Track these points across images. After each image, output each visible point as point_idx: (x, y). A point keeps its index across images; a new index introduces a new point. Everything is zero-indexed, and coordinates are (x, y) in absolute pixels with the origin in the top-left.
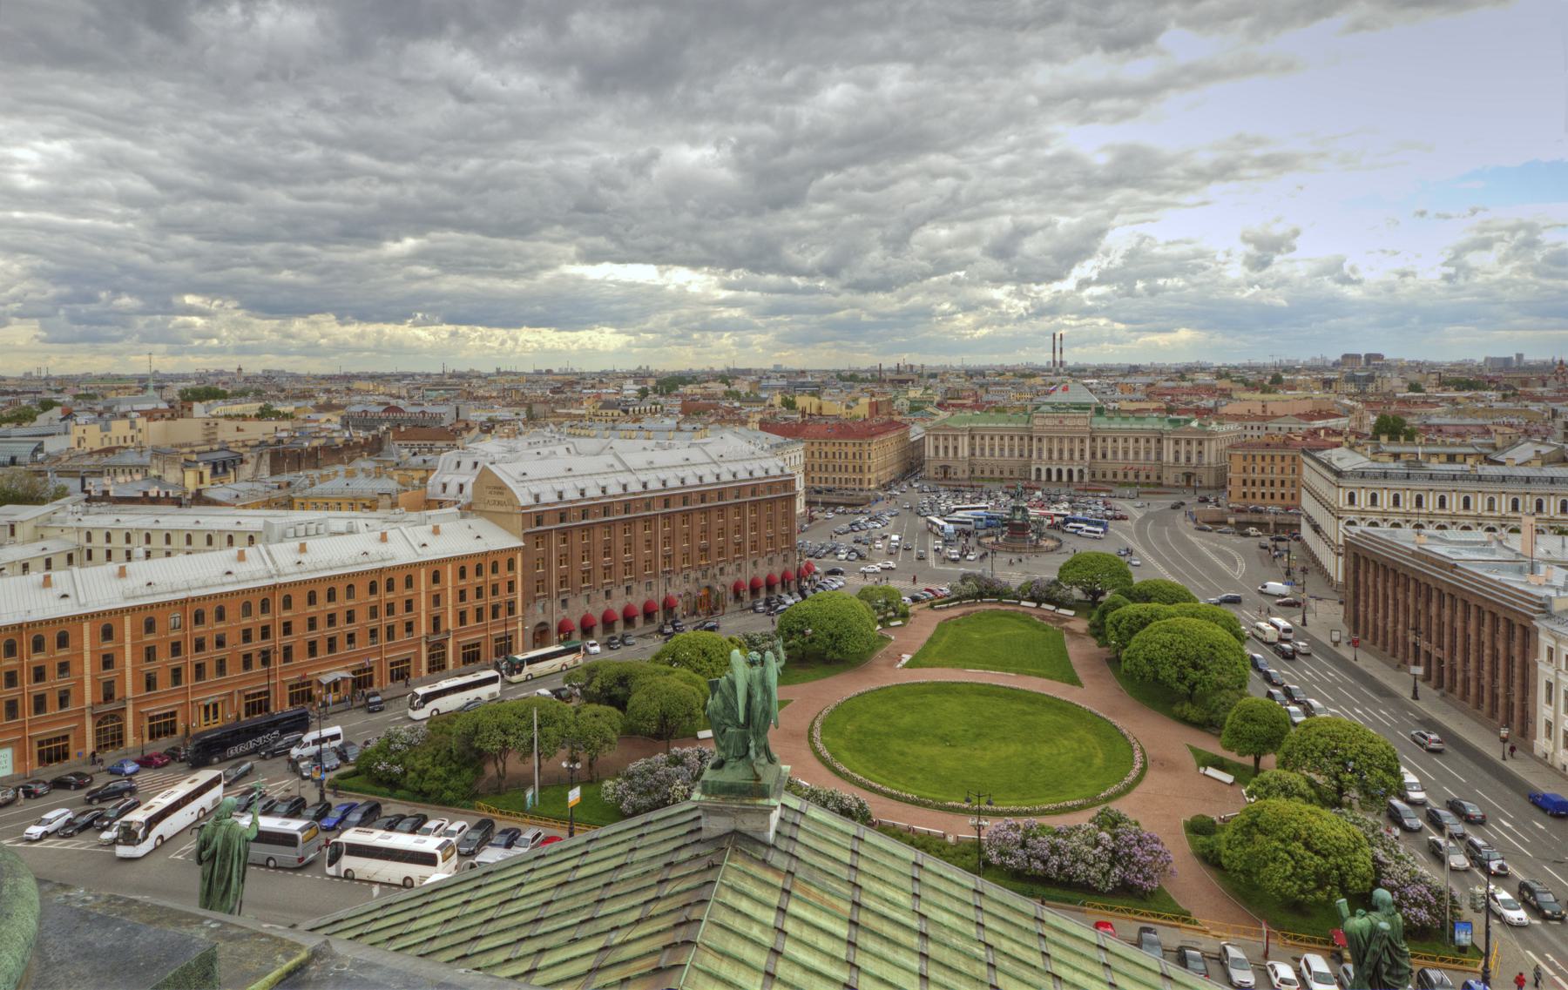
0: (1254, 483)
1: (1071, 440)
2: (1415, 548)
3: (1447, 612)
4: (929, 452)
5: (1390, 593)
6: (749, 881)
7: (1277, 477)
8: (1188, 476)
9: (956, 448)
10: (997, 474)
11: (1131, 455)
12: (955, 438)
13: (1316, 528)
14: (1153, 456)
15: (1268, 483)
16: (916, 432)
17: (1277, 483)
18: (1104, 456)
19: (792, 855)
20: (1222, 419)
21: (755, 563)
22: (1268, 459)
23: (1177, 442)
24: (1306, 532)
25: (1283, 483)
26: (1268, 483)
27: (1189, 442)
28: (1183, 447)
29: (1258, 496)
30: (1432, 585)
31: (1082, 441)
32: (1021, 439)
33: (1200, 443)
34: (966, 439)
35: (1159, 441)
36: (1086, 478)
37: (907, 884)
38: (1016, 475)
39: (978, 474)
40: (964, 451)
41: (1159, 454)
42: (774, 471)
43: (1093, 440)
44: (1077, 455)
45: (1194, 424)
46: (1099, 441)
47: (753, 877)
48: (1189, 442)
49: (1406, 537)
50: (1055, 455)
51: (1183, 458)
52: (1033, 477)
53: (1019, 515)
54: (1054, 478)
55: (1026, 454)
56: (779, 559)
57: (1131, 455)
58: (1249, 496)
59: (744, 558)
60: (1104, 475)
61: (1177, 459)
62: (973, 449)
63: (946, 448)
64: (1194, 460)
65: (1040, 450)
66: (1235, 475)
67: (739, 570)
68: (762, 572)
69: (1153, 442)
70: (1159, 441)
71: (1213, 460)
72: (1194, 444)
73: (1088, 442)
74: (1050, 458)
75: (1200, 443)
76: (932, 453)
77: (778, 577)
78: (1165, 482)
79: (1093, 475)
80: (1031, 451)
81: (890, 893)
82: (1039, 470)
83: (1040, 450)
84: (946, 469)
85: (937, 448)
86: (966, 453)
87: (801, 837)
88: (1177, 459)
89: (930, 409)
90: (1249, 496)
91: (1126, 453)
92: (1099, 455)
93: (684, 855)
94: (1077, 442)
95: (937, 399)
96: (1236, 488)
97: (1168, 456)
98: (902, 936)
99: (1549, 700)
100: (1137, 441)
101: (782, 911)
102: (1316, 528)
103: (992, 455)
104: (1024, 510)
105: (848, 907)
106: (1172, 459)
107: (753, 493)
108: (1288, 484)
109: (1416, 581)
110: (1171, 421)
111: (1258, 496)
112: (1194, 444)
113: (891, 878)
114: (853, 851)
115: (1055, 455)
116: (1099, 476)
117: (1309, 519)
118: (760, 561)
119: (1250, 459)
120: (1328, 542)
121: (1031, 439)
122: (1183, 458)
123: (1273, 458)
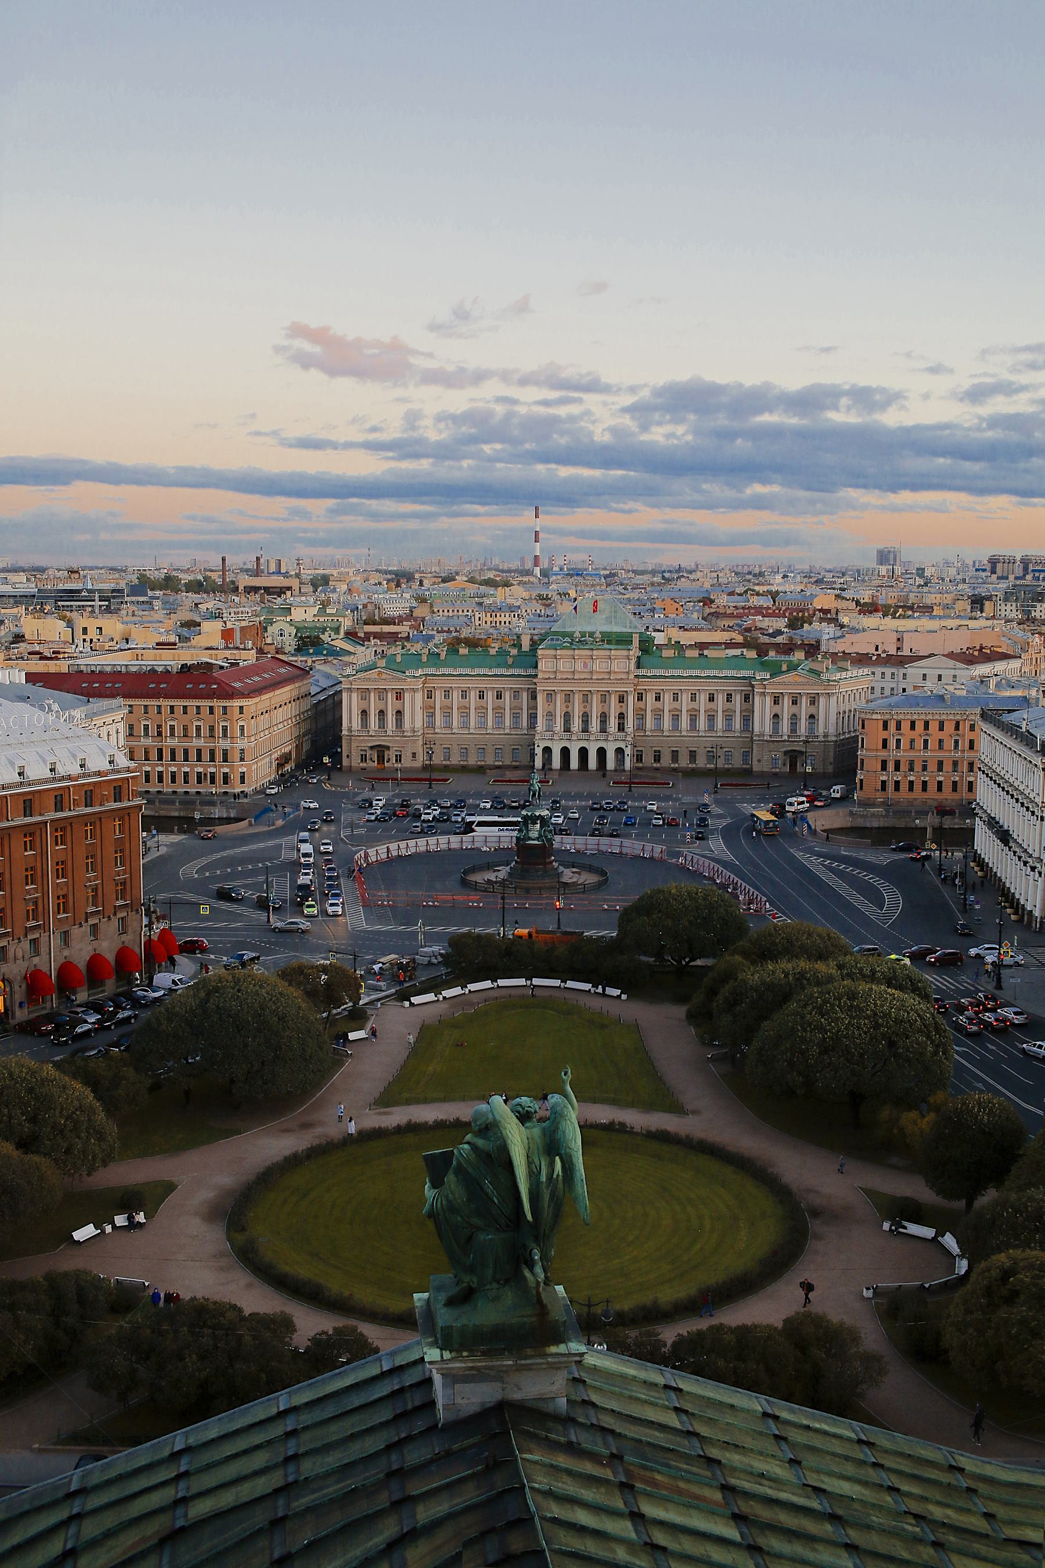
0: (897, 768)
1: (604, 697)
4: (350, 720)
6: (565, 1478)
7: (932, 755)
8: (793, 756)
11: (702, 723)
12: (399, 695)
13: (1005, 837)
14: (737, 723)
15: (918, 767)
17: (932, 767)
19: (603, 1429)
21: (66, 936)
22: (920, 726)
23: (776, 701)
24: (985, 842)
25: (940, 764)
28: (786, 708)
29: (904, 787)
31: (621, 700)
32: (516, 693)
33: (813, 701)
34: (419, 696)
36: (628, 765)
37: (771, 1446)
41: (747, 719)
42: (98, 763)
44: (613, 724)
47: (569, 1473)
50: (576, 725)
51: (785, 727)
52: (538, 763)
53: (535, 831)
54: (574, 764)
55: (525, 724)
56: (110, 928)
57: (702, 723)
58: (890, 787)
59: (45, 928)
63: (382, 713)
65: (550, 715)
66: (869, 754)
67: (37, 953)
68: (81, 952)
69: (738, 699)
71: (832, 730)
72: (804, 701)
73: (631, 699)
74: (567, 730)
76: (356, 724)
77: (111, 957)
78: (756, 768)
79: (639, 758)
81: (760, 1465)
82: (547, 750)
83: (550, 715)
84: (381, 750)
85: (364, 713)
86: (419, 724)
87: (595, 1398)
89: (340, 644)
90: (890, 787)
91: (693, 718)
93: (414, 1455)
94: (614, 700)
95: (347, 623)
96: (869, 774)
98: (811, 1526)
101: (637, 1517)
102: (1005, 837)
103: (466, 726)
105: (718, 1496)
106: (768, 729)
107: (59, 806)
108: (948, 767)
110: (764, 666)
111: (904, 787)
112: (804, 701)
113: (748, 1442)
114: (677, 1409)
115: (576, 725)
116: (648, 760)
117: (992, 823)
118: (76, 932)
119: (892, 726)
121: (534, 697)
123: (927, 725)
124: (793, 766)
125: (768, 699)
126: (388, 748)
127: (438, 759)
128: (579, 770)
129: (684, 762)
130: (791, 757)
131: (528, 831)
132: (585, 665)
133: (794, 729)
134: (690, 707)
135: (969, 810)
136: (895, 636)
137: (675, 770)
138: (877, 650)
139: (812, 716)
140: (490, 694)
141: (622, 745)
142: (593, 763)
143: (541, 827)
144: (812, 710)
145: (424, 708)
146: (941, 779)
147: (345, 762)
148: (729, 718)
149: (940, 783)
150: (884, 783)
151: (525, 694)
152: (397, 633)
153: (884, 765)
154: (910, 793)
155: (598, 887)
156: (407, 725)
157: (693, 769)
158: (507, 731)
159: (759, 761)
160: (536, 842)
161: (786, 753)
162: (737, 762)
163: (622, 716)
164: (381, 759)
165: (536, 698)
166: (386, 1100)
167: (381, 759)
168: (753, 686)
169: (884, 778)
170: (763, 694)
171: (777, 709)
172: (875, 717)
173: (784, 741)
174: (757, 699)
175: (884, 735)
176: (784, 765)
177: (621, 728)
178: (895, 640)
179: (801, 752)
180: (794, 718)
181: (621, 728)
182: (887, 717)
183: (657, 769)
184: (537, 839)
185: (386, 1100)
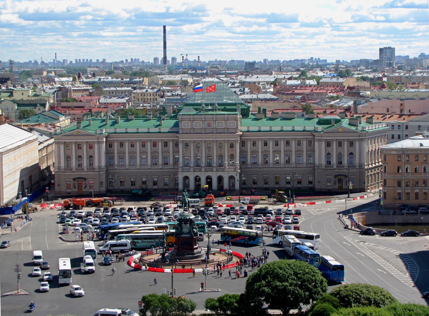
8: (340, 178)
9: (91, 157)
12: (91, 147)
23: (328, 144)
26: (421, 184)
27: (340, 144)
29: (412, 196)
31: (232, 146)
32: (166, 144)
33: (351, 144)
35: (310, 143)
36: (237, 186)
38: (160, 185)
43: (243, 144)
45: (345, 123)
46: (249, 145)
48: (340, 144)
51: (334, 161)
52: (181, 187)
55: (171, 162)
61: (329, 163)
62: (109, 154)
63: (80, 157)
69: (304, 144)
70: (310, 143)
72: (346, 144)
75: (351, 144)
82: (186, 178)
85: (68, 158)
86: (103, 164)
88: (329, 163)
94: (226, 147)
97: (320, 158)
104: (191, 221)
106: (323, 162)
112: (346, 145)
121: (177, 145)
122: (334, 161)
125: (323, 144)
126: (85, 179)
127: (117, 186)
132: (209, 125)
136: (400, 102)
139: (351, 154)
140: (149, 144)
141: (233, 174)
143: (190, 226)
144: (351, 150)
145: (107, 153)
150: (399, 194)
151: (171, 144)
154: (417, 200)
156: (96, 164)
158: (161, 167)
159: (319, 182)
160: (187, 235)
161: (336, 176)
162: (305, 184)
163: (232, 157)
165: (178, 147)
167: (80, 186)
168: (314, 136)
169: (399, 191)
170: (320, 140)
171: (329, 149)
172: (393, 153)
173: (335, 169)
174: (316, 144)
175: (399, 164)
176: (335, 184)
178: (399, 105)
179: (346, 176)
180: (340, 156)
182: (400, 153)
184: (188, 233)
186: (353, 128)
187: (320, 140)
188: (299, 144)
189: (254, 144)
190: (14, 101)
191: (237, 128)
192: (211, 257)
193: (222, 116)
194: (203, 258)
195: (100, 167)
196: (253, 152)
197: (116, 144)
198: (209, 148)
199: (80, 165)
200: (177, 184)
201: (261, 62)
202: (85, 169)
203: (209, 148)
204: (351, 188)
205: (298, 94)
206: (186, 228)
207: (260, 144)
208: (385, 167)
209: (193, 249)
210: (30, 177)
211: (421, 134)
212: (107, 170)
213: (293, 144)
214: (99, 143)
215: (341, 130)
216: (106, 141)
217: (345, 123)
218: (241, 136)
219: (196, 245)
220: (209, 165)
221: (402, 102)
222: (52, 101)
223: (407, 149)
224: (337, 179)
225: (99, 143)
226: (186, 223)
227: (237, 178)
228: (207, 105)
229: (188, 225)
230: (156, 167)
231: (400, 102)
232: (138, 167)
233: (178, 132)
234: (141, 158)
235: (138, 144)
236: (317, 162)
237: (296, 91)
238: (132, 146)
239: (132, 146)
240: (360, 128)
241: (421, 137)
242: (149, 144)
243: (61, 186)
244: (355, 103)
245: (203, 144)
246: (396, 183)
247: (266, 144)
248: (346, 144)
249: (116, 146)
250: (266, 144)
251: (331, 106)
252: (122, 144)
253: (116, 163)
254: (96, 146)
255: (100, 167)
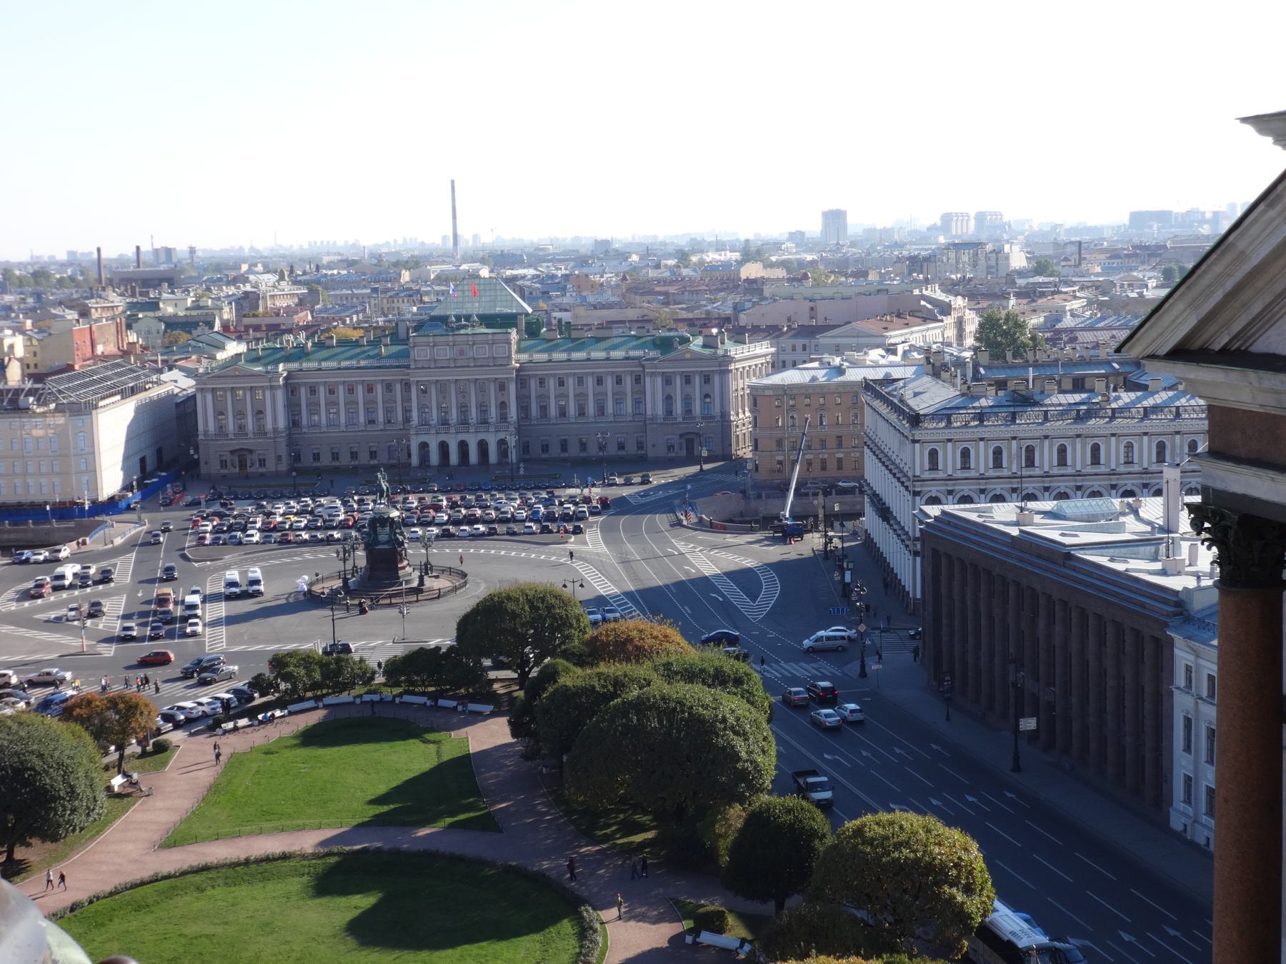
2: (1014, 531)
3: (1058, 629)
4: (206, 422)
5: (983, 608)
9: (259, 413)
10: (345, 460)
14: (629, 406)
16: (176, 382)
17: (832, 443)
18: (544, 409)
20: (739, 335)
23: (668, 380)
27: (688, 380)
30: (1038, 587)
31: (502, 387)
32: (389, 387)
33: (707, 379)
34: (280, 396)
35: (638, 380)
36: (513, 456)
39: (307, 461)
40: (277, 419)
41: (639, 402)
45: (697, 343)
46: (533, 384)
48: (688, 380)
49: (1002, 516)
51: (678, 408)
52: (415, 460)
54: (454, 458)
55: (400, 418)
57: (591, 409)
60: (545, 448)
61: (669, 412)
62: (292, 406)
63: (240, 414)
64: (697, 408)
69: (628, 381)
70: (638, 380)
72: (697, 380)
73: (512, 388)
76: (211, 427)
78: (651, 453)
79: (524, 448)
80: (407, 411)
82: (424, 446)
83: (422, 408)
84: (242, 455)
85: (220, 413)
86: (282, 423)
88: (669, 412)
92: (534, 411)
94: (492, 389)
97: (654, 405)
99: (1188, 748)
100: (600, 381)
102: (885, 513)
106: (660, 411)
109: (1018, 584)
116: (536, 451)
120: (901, 533)
121: (407, 386)
122: (678, 408)
124: (690, 449)
125: (659, 380)
126: (251, 451)
127: (307, 461)
128: (460, 465)
129: (574, 451)
130: (687, 440)
131: (376, 534)
132: (462, 352)
133: (688, 411)
134: (578, 392)
135: (861, 487)
136: (808, 304)
137: (565, 460)
138: (789, 320)
140: (360, 388)
141: (501, 436)
142: (474, 457)
144: (707, 389)
146: (840, 455)
147: (204, 469)
148: (618, 400)
149: (840, 461)
150: (780, 463)
151: (398, 387)
152: (278, 325)
153: (780, 443)
155: (455, 589)
156: (269, 426)
157: (336, 468)
161: (681, 436)
162: (631, 449)
163: (503, 405)
164: (242, 464)
166: (172, 841)
167: (242, 464)
168: (643, 367)
169: (780, 458)
172: (767, 393)
174: (648, 379)
177: (503, 418)
178: (808, 309)
179: (699, 435)
180: (687, 401)
181: (503, 418)
182: (781, 392)
183: (545, 460)
185: (172, 841)
186: (707, 351)
187: (652, 374)
188: (619, 381)
189: (542, 382)
190: (160, 319)
191: (509, 357)
192: (428, 582)
193: (484, 337)
194: (415, 584)
195: (275, 430)
196: (539, 397)
197: (303, 390)
198: (462, 393)
199: (241, 427)
200: (409, 456)
201: (241, 248)
202: (251, 435)
203: (462, 393)
204: (705, 453)
205: (660, 293)
206: (384, 534)
207: (552, 383)
208: (755, 418)
209: (396, 569)
210: (159, 451)
211: (820, 360)
212: (289, 436)
213: (609, 382)
214: (272, 388)
215: (688, 356)
216: (286, 384)
217: (697, 343)
218: (518, 370)
219: (401, 561)
220: (464, 422)
221: (812, 304)
222: (226, 317)
223: (792, 387)
224: (683, 441)
225: (272, 388)
226: (383, 526)
227: (512, 441)
228: (458, 318)
229: (387, 529)
230: (370, 427)
231: (808, 304)
232: (343, 429)
233: (408, 367)
234: (328, 412)
235: (341, 388)
236: (649, 412)
237: (657, 289)
238: (332, 392)
239: (332, 392)
240: (720, 352)
241: (816, 364)
242: (360, 388)
243: (210, 465)
244: (735, 308)
245: (453, 386)
246: (774, 444)
247: (561, 383)
248: (697, 380)
249: (303, 392)
250: (561, 383)
251: (708, 312)
252: (313, 390)
253: (305, 422)
254: (268, 393)
255: (275, 430)
